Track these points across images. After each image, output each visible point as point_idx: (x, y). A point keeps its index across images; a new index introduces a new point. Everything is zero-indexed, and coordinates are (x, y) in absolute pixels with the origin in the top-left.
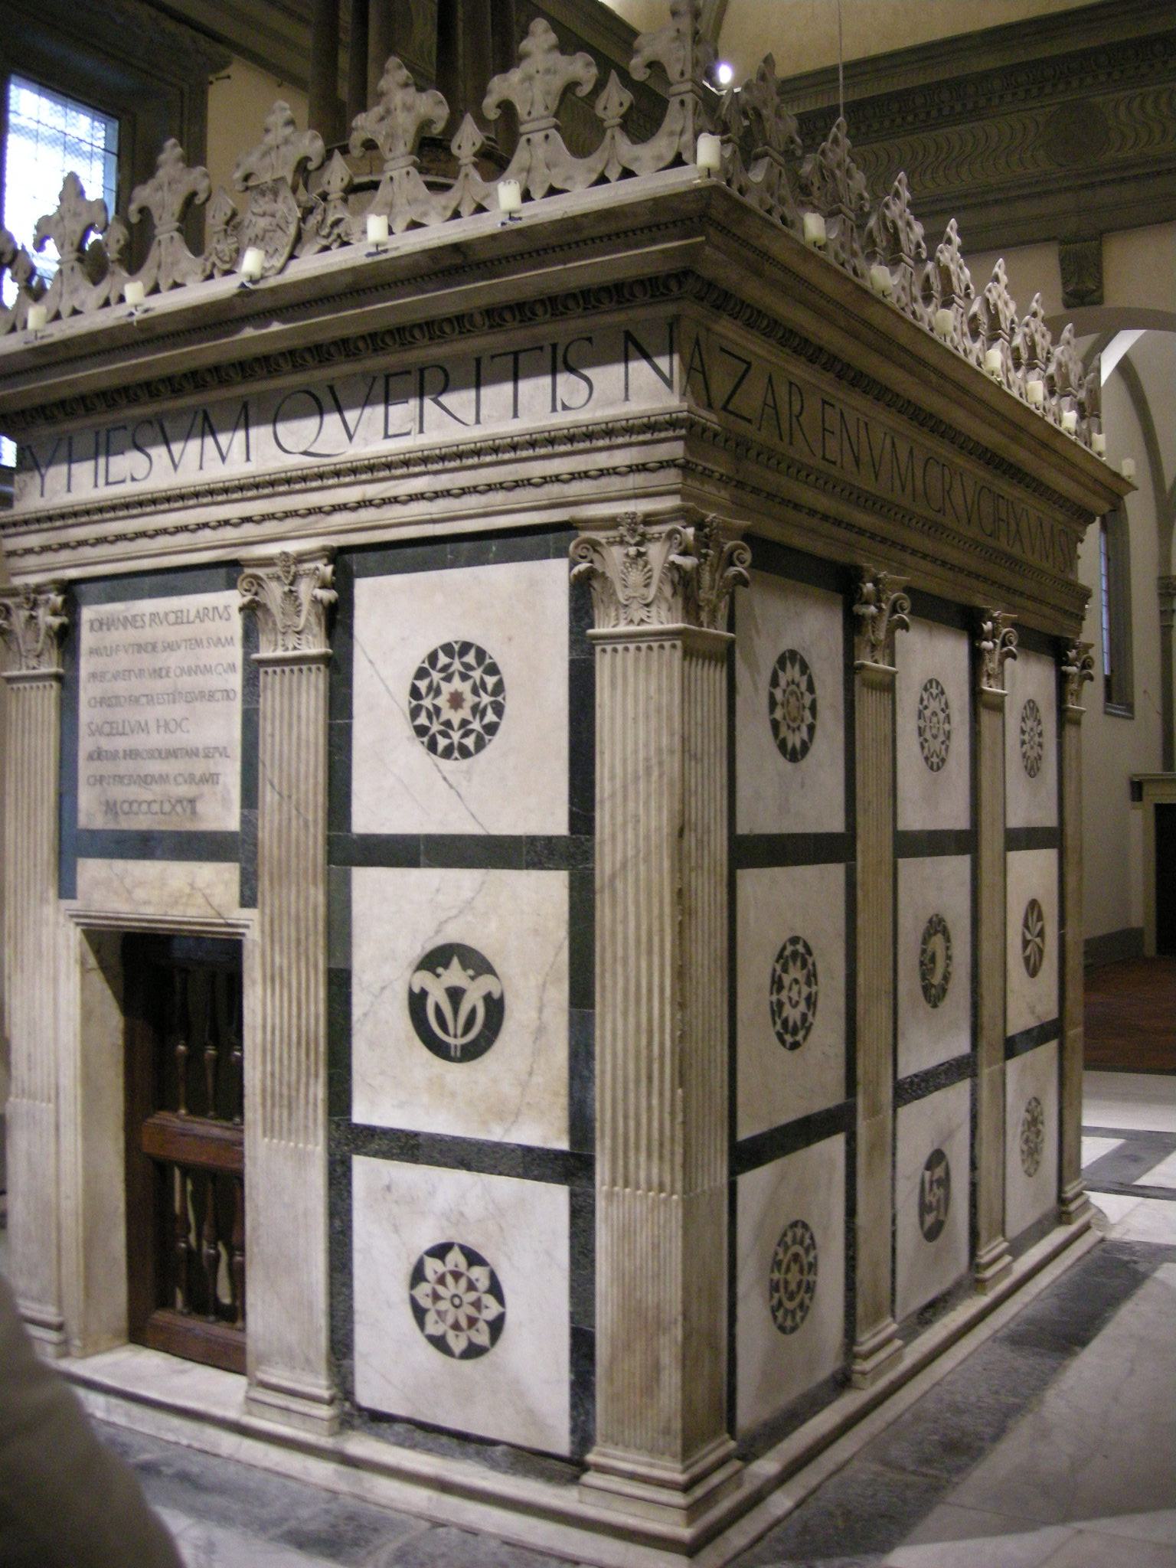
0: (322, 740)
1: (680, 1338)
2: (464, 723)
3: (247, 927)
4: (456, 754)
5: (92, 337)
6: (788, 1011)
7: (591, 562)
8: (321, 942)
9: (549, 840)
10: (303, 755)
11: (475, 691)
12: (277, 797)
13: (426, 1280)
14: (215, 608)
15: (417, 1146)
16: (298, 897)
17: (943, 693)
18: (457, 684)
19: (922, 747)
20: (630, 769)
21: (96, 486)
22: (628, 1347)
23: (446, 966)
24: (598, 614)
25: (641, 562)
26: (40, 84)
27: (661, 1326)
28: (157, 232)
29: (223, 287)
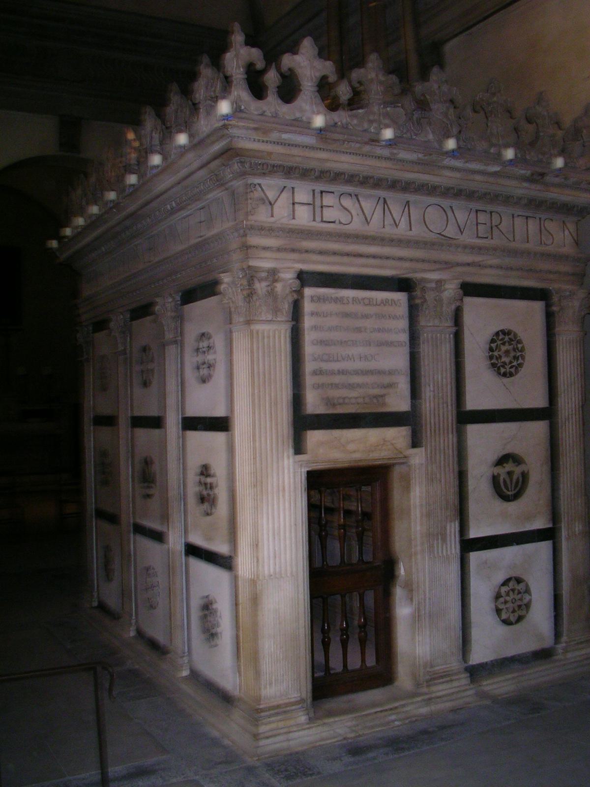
2: (511, 362)
13: (502, 597)
20: (569, 382)
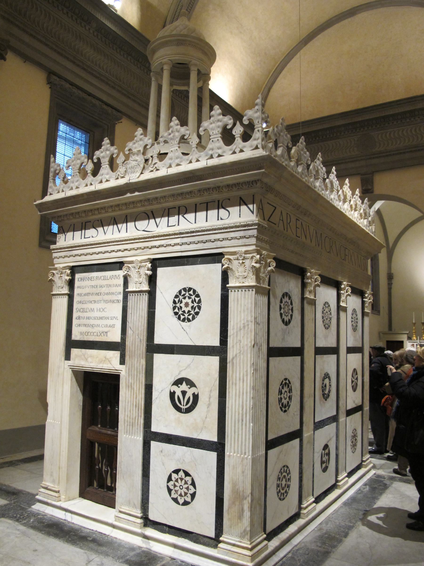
0: (146, 316)
1: (250, 501)
2: (189, 311)
3: (122, 371)
4: (186, 321)
5: (82, 195)
6: (283, 400)
7: (228, 265)
8: (144, 376)
10: (140, 320)
11: (192, 302)
12: (132, 332)
13: (172, 481)
14: (116, 276)
16: (137, 362)
17: (329, 306)
18: (187, 300)
19: (323, 322)
22: (234, 503)
23: (181, 384)
24: (230, 280)
25: (243, 265)
26: (67, 122)
28: (102, 165)
29: (122, 182)
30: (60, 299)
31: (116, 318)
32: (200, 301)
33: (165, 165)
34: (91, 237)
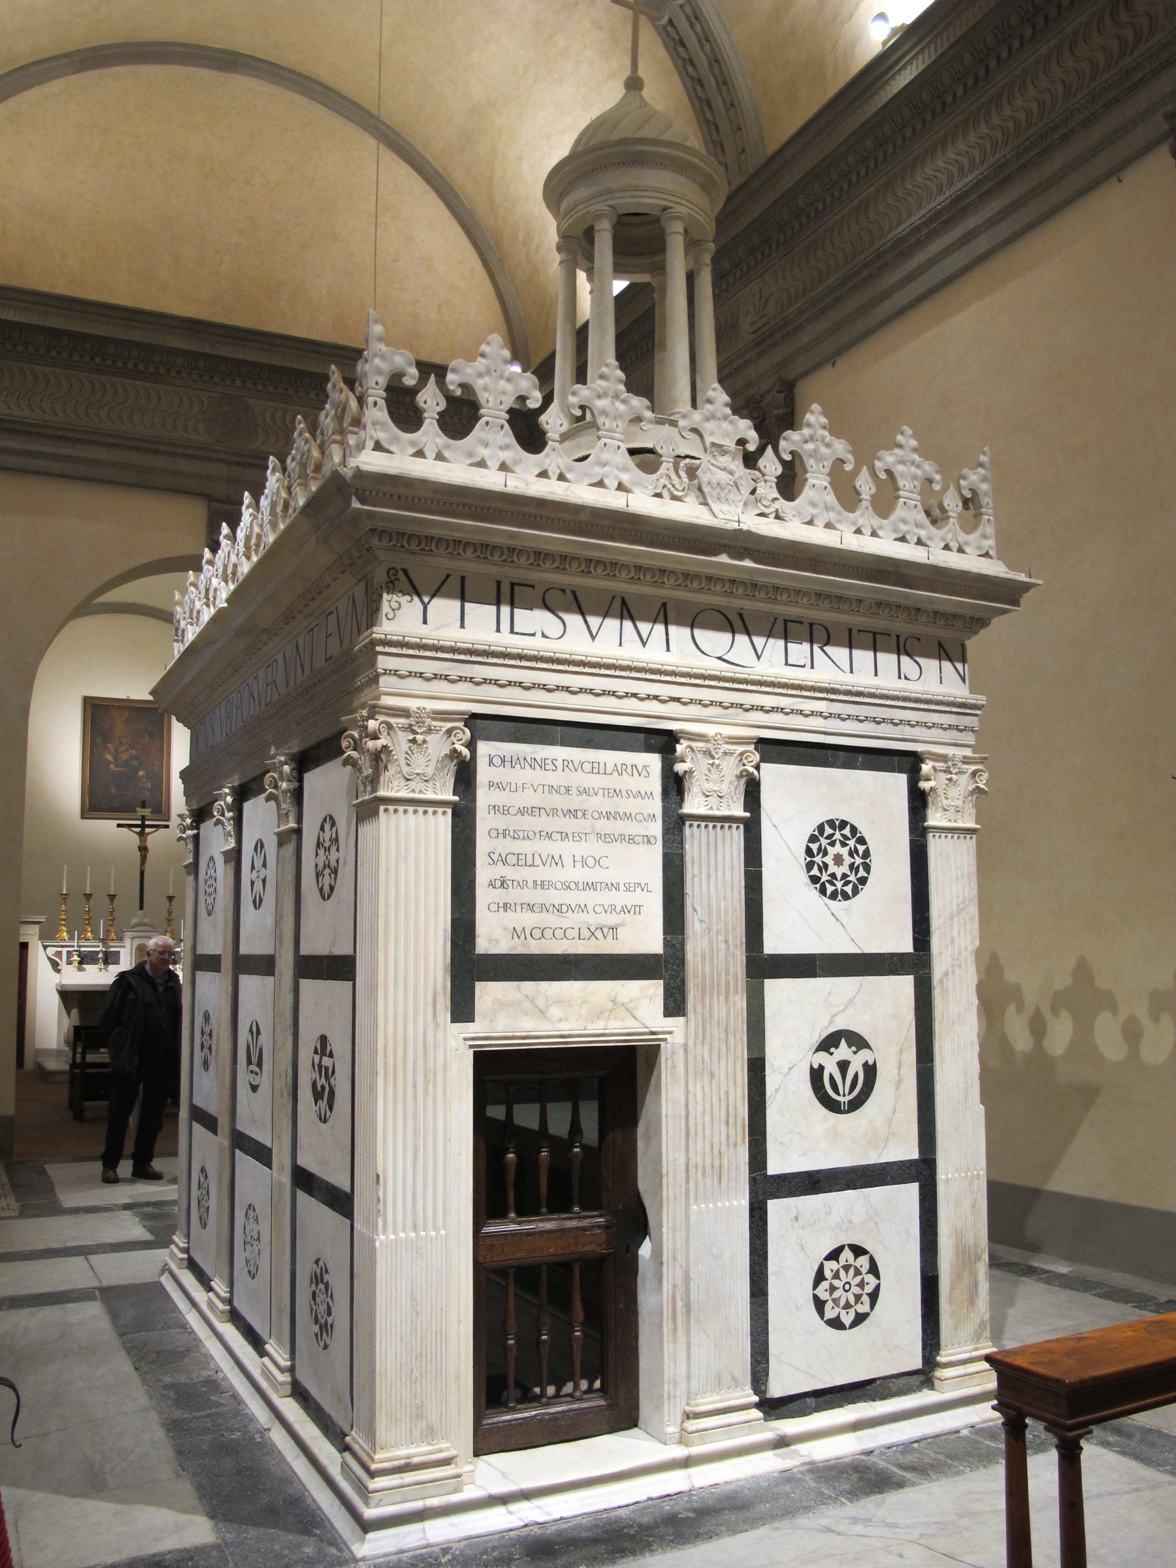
2: (844, 876)
3: (670, 1033)
4: (839, 897)
9: (902, 956)
11: (851, 854)
14: (634, 766)
15: (818, 1182)
18: (838, 848)
21: (498, 630)
23: (837, 1047)
27: (979, 1258)
30: (393, 817)
31: (644, 887)
32: (867, 854)
33: (800, 513)
34: (539, 634)
